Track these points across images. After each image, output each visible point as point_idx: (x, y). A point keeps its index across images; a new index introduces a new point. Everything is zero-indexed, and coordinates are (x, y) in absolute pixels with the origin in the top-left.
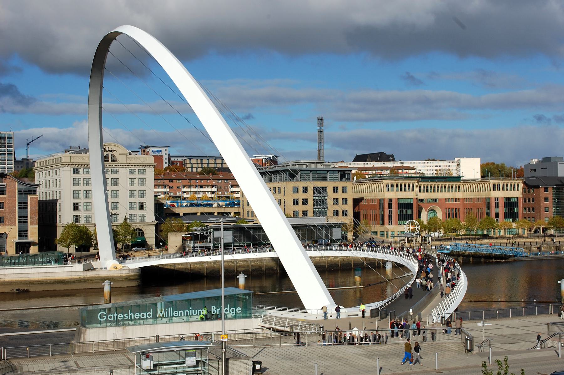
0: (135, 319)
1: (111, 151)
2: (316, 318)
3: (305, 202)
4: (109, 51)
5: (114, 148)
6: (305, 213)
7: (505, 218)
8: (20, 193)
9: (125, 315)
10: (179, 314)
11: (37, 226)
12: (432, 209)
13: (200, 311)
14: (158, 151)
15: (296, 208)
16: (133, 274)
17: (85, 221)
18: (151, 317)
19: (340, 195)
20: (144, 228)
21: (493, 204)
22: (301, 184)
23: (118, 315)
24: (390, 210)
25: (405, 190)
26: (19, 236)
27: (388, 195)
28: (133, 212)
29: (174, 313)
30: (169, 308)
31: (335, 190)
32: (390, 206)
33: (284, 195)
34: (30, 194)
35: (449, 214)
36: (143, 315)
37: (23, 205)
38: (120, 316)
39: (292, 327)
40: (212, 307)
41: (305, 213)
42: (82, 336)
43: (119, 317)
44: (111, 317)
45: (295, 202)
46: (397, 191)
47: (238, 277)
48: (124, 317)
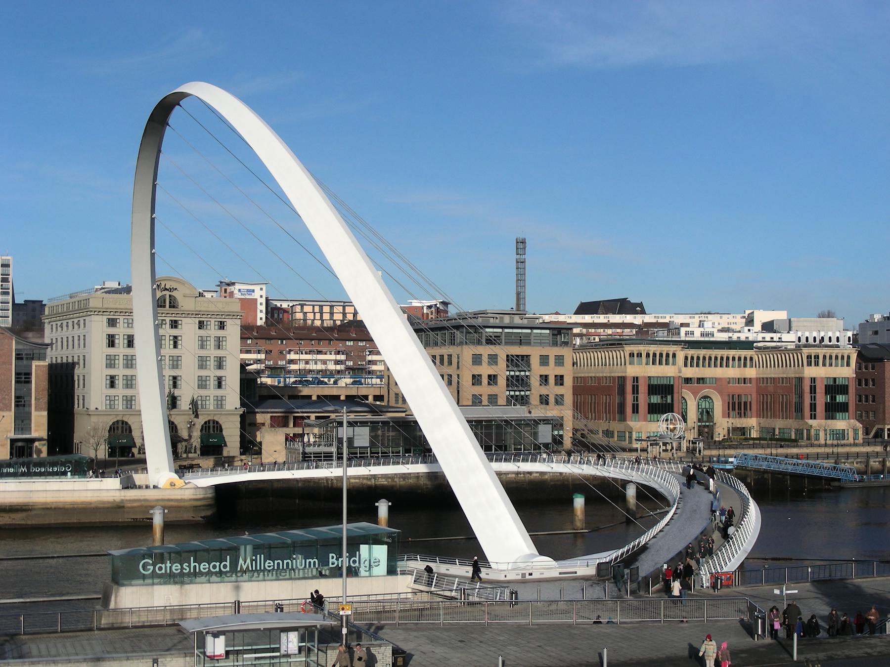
0: (201, 574)
1: (170, 290)
2: (506, 576)
3: (492, 379)
4: (168, 124)
5: (174, 285)
6: (493, 399)
7: (649, 413)
8: (19, 357)
9: (185, 565)
10: (274, 566)
11: (45, 413)
12: (705, 394)
13: (310, 562)
14: (248, 291)
15: (477, 390)
16: (201, 496)
18: (228, 569)
19: (552, 371)
20: (222, 420)
21: (807, 389)
22: (485, 351)
23: (172, 565)
24: (635, 395)
25: (660, 363)
27: (633, 370)
28: (203, 392)
29: (267, 565)
30: (258, 556)
31: (544, 360)
32: (635, 390)
33: (458, 368)
35: (734, 404)
36: (215, 567)
37: (23, 378)
38: (176, 568)
39: (464, 591)
40: (331, 555)
41: (493, 399)
42: (113, 598)
43: (174, 568)
44: (160, 569)
45: (476, 379)
46: (647, 364)
47: (377, 504)
48: (182, 568)
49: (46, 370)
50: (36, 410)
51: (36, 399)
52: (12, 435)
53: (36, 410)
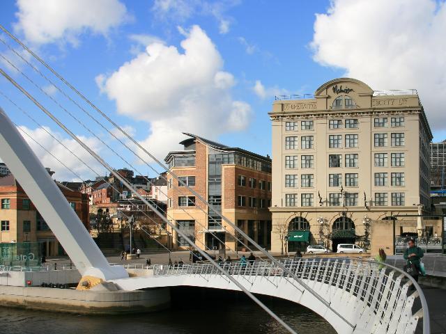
1: (347, 91)
5: (349, 86)
17: (288, 204)
26: (210, 225)
52: (206, 230)
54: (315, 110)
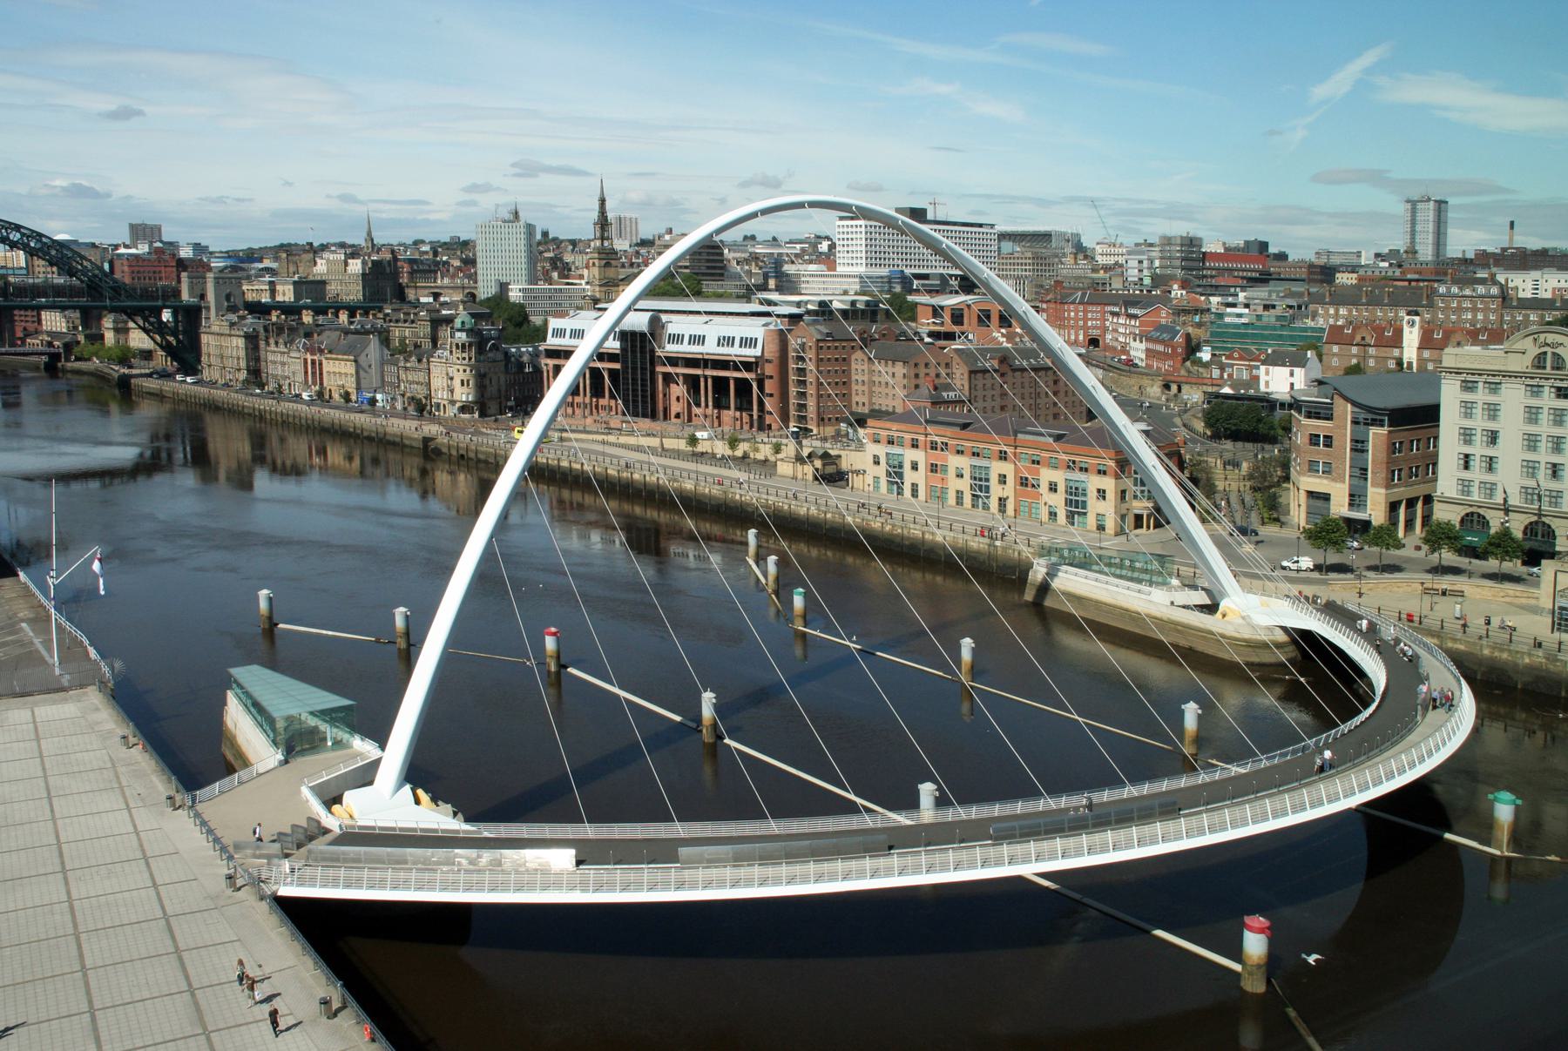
8: (1355, 422)
26: (1350, 505)
34: (1372, 425)
49: (1384, 439)
50: (1372, 486)
51: (1372, 472)
53: (1372, 486)
54: (1502, 368)
